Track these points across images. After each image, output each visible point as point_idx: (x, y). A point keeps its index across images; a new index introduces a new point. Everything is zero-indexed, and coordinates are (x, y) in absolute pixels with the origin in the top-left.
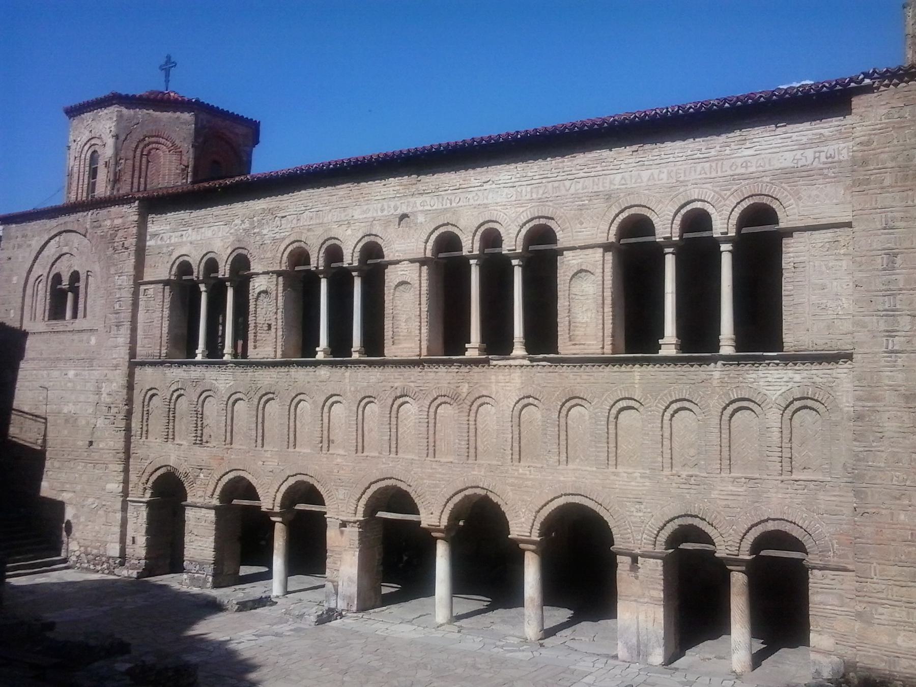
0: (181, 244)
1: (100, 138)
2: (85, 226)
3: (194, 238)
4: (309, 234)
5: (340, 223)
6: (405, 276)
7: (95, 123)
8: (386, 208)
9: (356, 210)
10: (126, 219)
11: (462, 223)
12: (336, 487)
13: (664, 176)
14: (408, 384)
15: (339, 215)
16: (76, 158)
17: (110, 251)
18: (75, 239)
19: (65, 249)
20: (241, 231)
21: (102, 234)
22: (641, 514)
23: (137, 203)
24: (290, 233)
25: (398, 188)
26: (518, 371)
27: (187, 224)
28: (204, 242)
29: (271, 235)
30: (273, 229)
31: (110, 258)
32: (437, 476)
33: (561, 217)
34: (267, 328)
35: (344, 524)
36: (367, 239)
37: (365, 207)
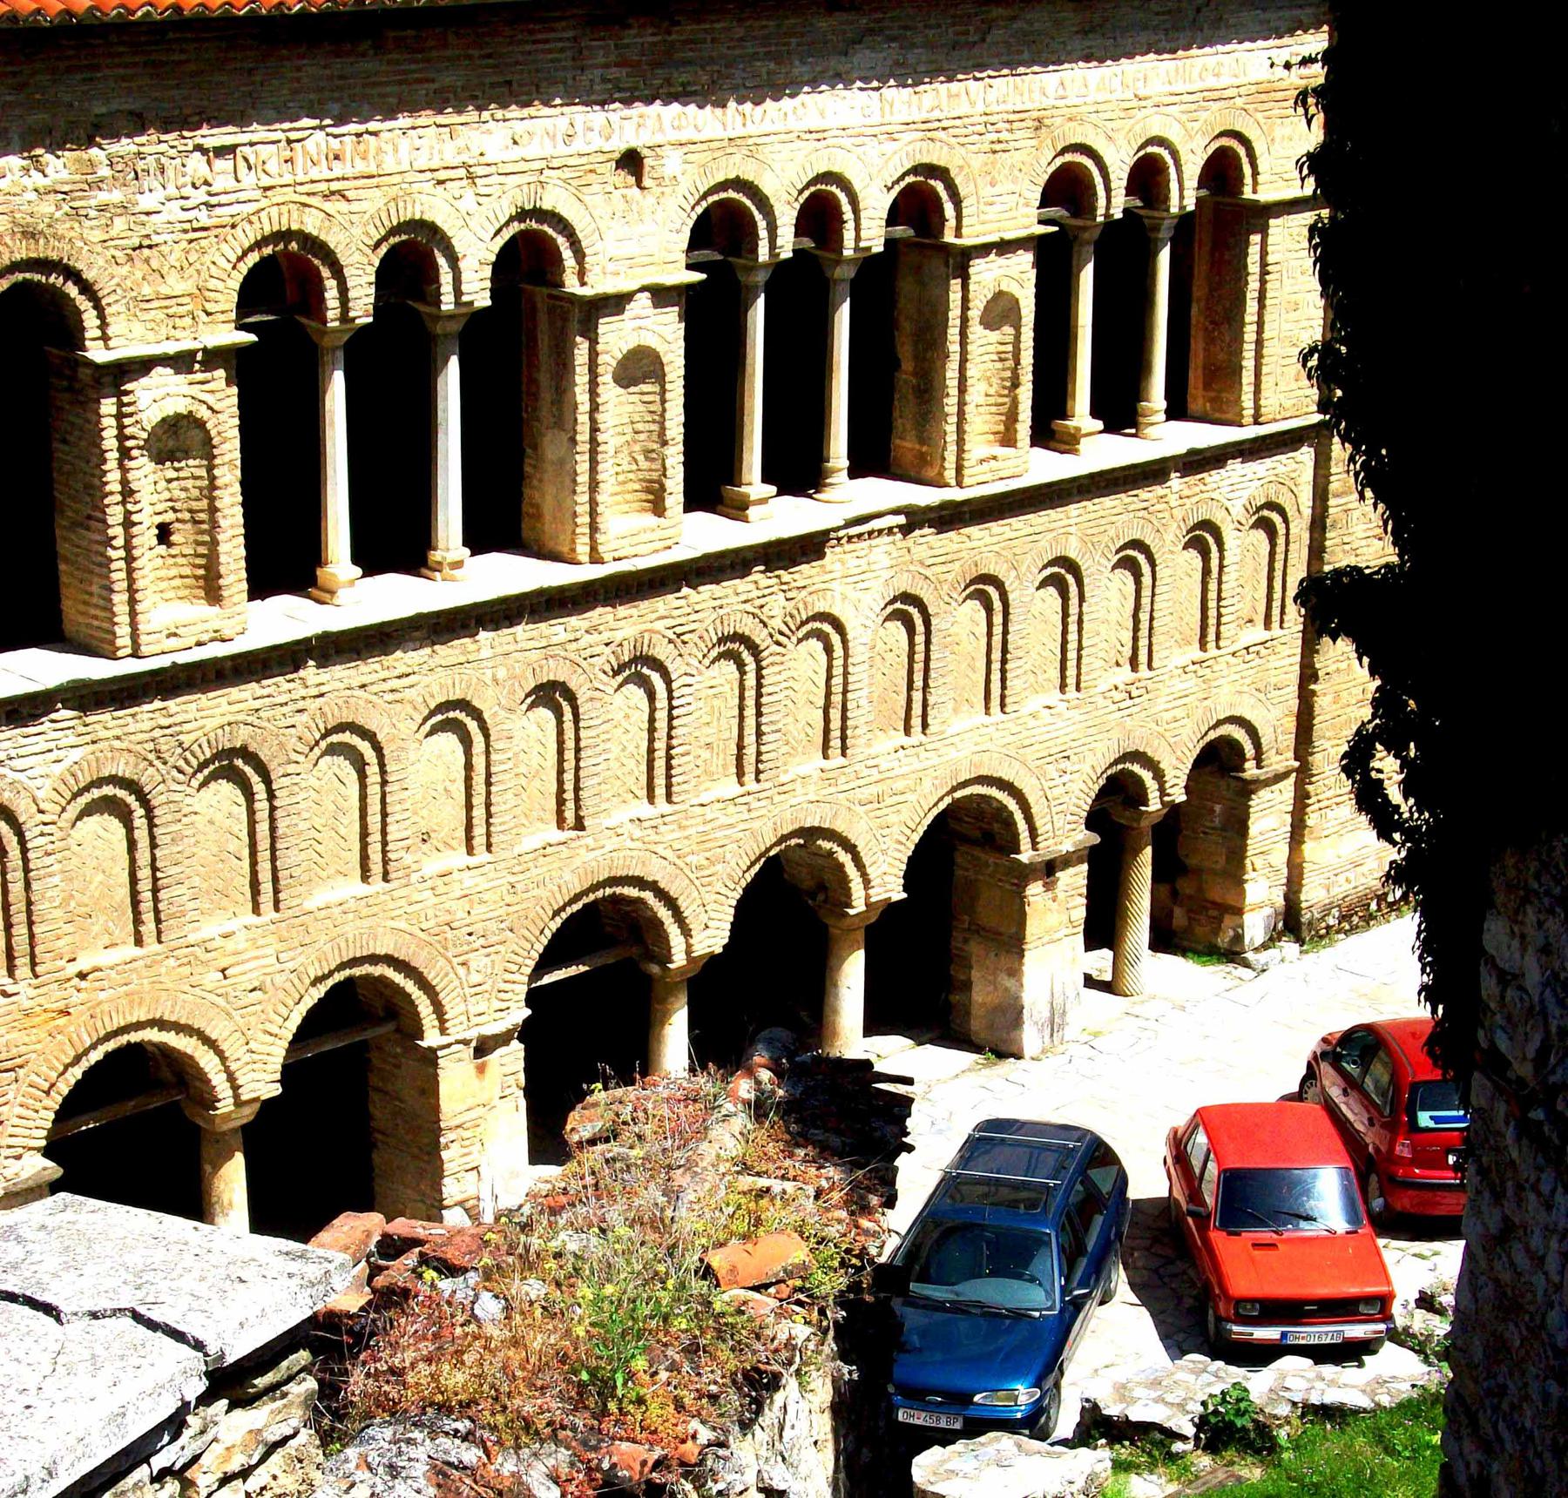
4: (332, 206)
5: (442, 175)
6: (643, 333)
8: (579, 127)
9: (489, 132)
11: (768, 187)
12: (461, 959)
13: (1116, 83)
14: (649, 626)
15: (437, 147)
22: (1066, 778)
24: (253, 207)
25: (614, 73)
26: (885, 539)
29: (173, 211)
30: (185, 192)
32: (719, 834)
33: (961, 168)
34: (155, 541)
35: (483, 1048)
36: (516, 227)
37: (519, 128)
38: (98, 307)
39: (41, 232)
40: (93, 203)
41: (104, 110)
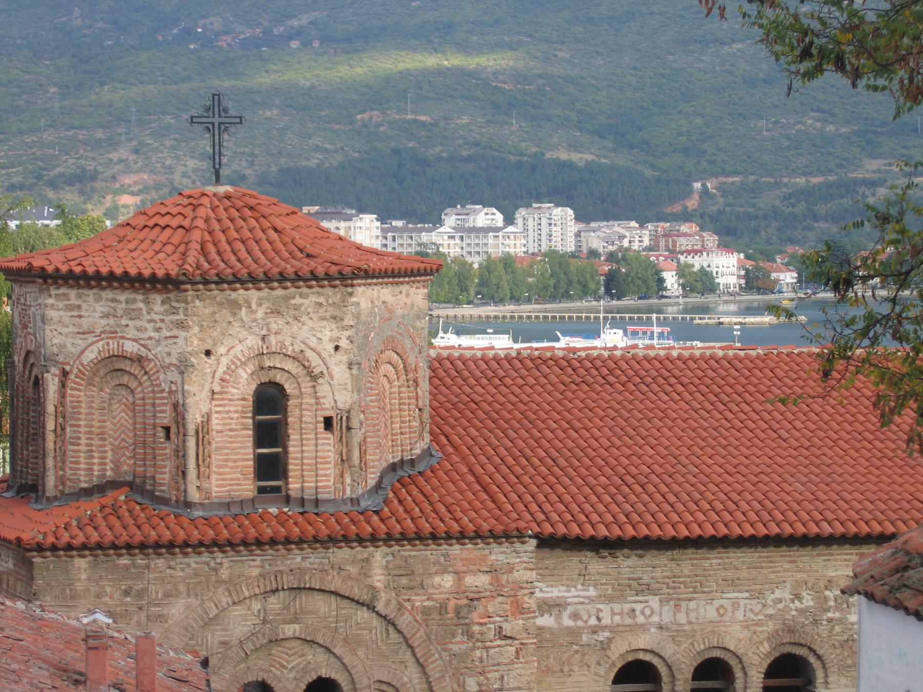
0: (635, 628)
1: (299, 358)
2: (368, 581)
3: (667, 618)
7: (281, 321)
10: (505, 577)
16: (213, 393)
17: (459, 645)
18: (322, 605)
19: (290, 630)
20: (794, 613)
21: (426, 603)
23: (534, 542)
27: (649, 590)
28: (696, 627)
31: (463, 657)
38: (824, 667)
39: (798, 631)
40: (825, 618)
41: (833, 574)
